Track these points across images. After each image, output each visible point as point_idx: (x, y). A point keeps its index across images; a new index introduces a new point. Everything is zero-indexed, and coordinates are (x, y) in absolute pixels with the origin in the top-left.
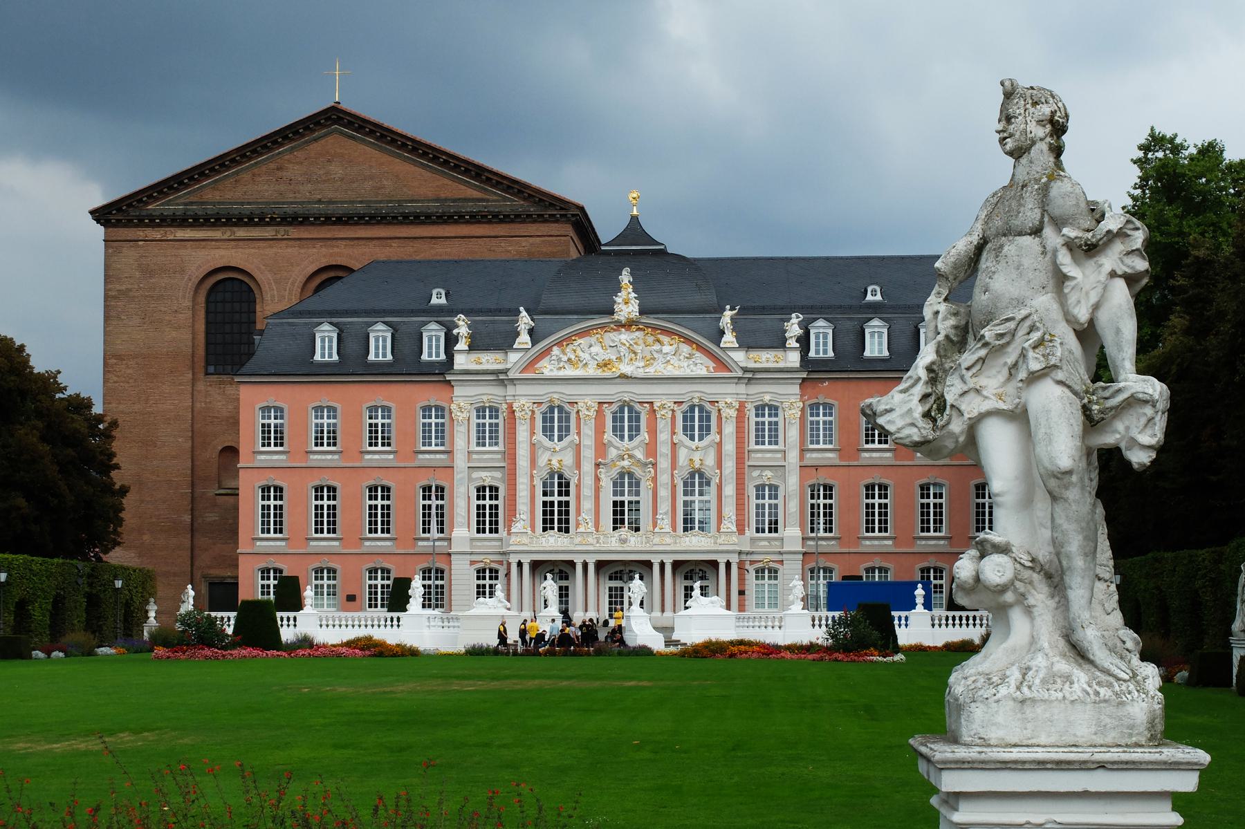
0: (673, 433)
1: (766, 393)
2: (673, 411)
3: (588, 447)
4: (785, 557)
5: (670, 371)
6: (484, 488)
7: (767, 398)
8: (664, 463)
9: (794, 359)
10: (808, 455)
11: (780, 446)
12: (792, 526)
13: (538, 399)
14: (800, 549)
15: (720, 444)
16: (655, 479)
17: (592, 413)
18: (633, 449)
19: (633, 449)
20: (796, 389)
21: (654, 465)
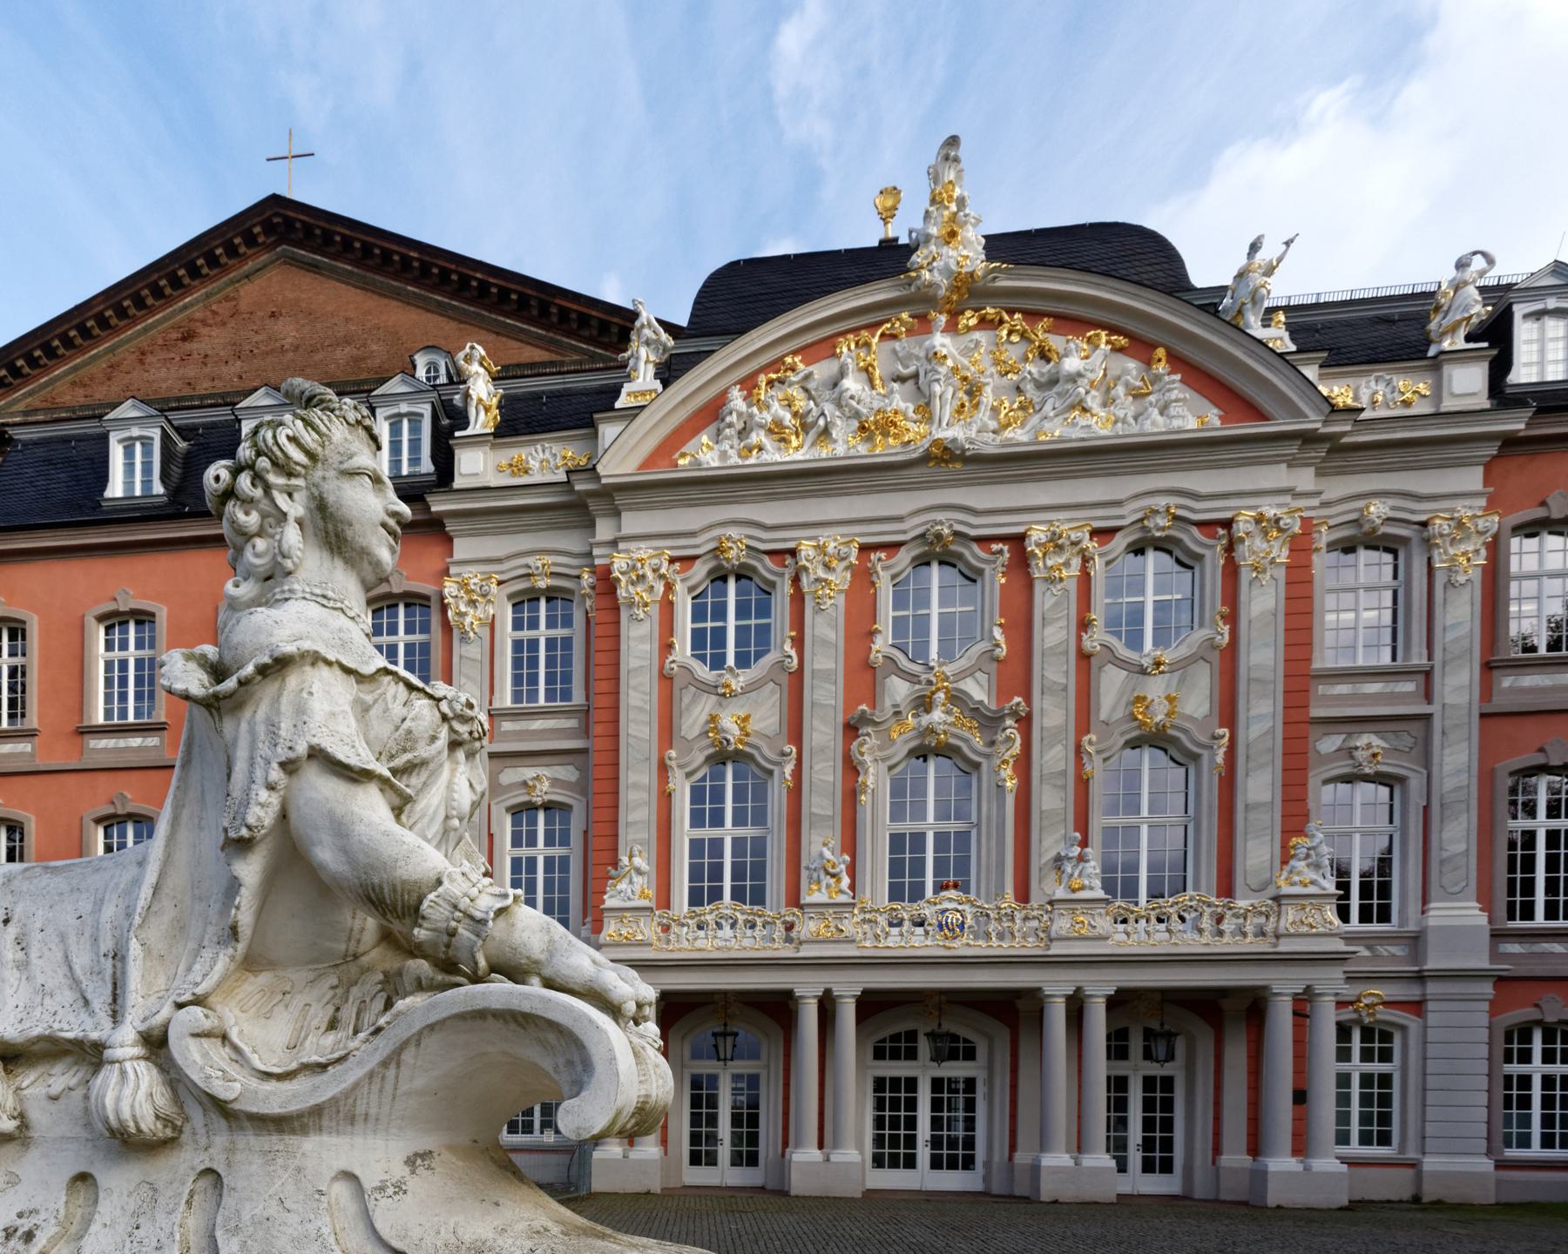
0: (1084, 625)
1: (1377, 497)
2: (1086, 560)
3: (827, 676)
4: (1433, 988)
5: (1098, 426)
6: (531, 808)
7: (1377, 510)
8: (1052, 714)
9: (1468, 382)
10: (1507, 682)
11: (1418, 659)
12: (1452, 896)
13: (685, 547)
14: (1482, 962)
15: (1230, 654)
16: (1024, 765)
17: (841, 578)
18: (962, 675)
19: (962, 675)
20: (1473, 479)
21: (1025, 722)
